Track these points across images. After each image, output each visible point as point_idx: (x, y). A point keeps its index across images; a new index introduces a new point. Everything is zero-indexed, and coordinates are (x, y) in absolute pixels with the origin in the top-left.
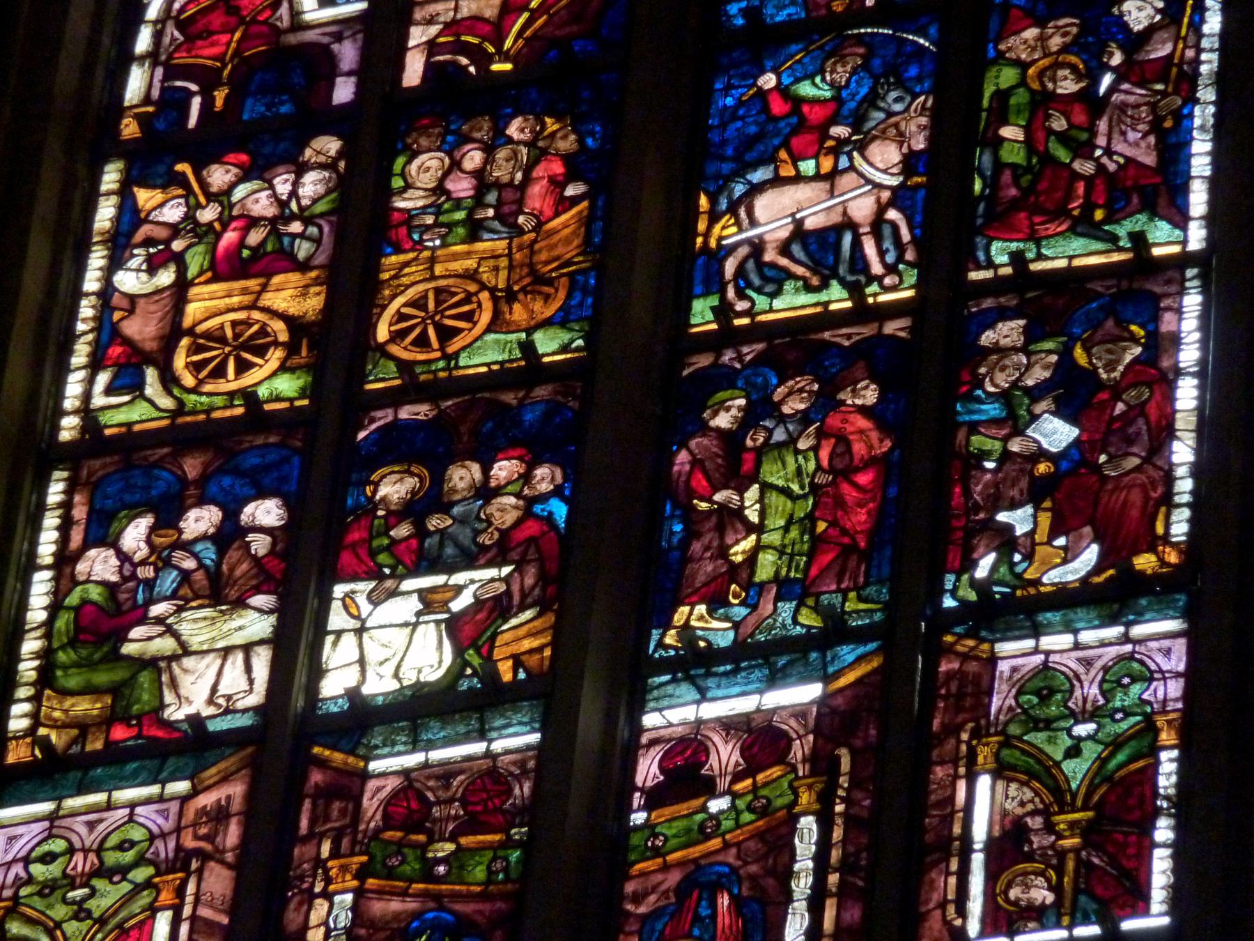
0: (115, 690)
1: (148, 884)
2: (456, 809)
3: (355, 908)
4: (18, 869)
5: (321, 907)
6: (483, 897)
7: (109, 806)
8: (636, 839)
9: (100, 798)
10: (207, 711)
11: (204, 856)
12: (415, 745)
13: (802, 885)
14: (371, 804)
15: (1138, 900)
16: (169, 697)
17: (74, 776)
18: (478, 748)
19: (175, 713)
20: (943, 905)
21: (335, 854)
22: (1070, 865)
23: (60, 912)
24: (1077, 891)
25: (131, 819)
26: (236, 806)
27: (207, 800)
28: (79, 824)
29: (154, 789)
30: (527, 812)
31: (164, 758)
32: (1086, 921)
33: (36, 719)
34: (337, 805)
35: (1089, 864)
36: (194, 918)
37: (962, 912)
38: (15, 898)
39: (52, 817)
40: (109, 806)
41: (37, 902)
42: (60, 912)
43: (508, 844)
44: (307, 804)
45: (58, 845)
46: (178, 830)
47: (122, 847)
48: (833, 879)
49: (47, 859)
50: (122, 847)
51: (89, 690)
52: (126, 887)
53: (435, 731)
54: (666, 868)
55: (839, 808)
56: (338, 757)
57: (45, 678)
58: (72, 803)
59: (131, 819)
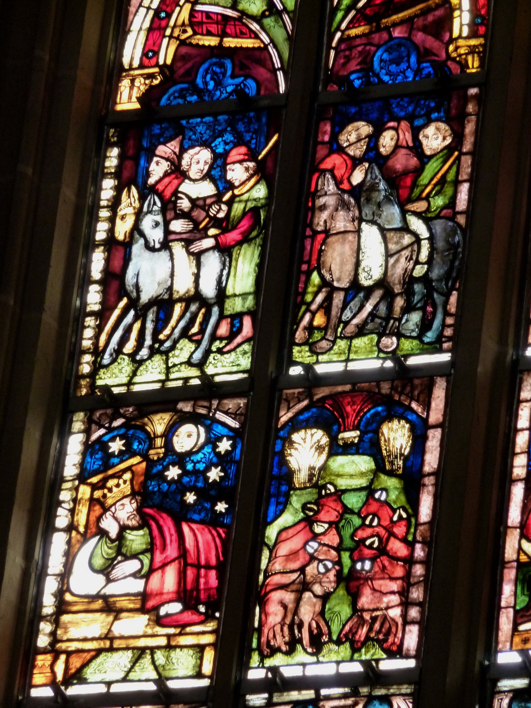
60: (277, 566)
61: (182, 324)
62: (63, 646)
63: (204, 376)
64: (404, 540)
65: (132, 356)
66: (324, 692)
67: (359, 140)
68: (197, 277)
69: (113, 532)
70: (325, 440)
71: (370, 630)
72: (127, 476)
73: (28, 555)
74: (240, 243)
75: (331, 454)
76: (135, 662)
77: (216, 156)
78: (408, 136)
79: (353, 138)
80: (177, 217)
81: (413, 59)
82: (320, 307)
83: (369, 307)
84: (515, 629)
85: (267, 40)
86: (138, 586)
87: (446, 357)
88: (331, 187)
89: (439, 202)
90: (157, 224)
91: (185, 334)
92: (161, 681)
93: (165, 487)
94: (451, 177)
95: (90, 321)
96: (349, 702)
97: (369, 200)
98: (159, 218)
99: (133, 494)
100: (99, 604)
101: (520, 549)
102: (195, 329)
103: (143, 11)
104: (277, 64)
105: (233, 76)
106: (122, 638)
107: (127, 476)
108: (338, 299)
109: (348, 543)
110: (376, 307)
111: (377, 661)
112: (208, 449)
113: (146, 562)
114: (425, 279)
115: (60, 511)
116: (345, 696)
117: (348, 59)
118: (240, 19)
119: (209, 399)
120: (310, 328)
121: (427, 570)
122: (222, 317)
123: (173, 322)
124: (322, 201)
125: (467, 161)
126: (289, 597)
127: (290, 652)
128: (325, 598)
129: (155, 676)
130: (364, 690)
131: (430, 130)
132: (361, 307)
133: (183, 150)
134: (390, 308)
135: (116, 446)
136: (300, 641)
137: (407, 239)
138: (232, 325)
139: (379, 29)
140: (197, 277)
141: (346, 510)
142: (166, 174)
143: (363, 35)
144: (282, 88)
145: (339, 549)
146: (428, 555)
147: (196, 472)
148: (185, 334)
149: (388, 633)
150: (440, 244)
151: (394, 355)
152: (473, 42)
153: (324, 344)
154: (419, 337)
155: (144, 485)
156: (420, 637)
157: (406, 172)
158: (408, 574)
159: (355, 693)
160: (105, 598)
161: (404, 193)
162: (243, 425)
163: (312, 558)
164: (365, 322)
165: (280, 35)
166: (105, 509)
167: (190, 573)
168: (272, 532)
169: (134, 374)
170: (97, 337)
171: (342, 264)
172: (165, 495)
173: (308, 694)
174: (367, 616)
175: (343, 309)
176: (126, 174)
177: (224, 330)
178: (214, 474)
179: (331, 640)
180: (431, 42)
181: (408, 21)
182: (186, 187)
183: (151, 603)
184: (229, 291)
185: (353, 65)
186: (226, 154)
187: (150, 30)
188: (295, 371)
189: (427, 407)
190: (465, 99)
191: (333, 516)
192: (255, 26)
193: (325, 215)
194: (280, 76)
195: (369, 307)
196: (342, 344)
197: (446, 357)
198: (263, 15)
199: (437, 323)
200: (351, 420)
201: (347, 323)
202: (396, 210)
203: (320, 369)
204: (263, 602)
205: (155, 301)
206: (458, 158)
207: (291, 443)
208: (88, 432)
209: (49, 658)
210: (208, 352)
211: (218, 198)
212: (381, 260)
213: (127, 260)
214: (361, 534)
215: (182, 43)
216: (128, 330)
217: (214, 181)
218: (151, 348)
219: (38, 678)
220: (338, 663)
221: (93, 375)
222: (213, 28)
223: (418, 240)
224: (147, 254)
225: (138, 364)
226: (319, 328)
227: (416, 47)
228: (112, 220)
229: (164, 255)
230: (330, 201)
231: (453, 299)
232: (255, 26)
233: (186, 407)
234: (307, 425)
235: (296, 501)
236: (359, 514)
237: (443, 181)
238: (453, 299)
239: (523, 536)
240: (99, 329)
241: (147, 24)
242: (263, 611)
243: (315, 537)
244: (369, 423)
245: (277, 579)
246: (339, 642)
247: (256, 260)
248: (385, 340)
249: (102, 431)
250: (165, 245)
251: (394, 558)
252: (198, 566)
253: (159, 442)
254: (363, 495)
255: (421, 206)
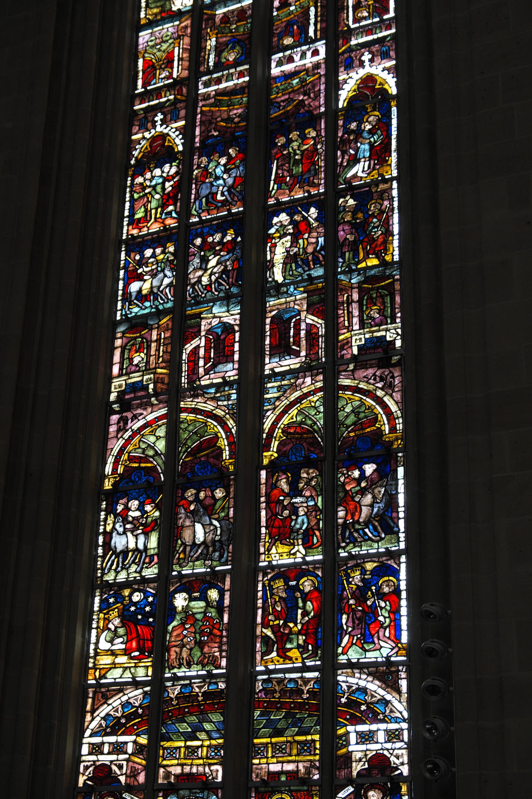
0: (162, 6)
1: (173, 43)
2: (236, 18)
3: (216, 41)
4: (146, 44)
5: (209, 42)
6: (243, 34)
7: (163, 29)
8: (275, 18)
9: (161, 28)
10: (181, 7)
11: (183, 36)
12: (225, 7)
13: (312, 21)
14: (217, 20)
15: (387, 11)
16: (173, 6)
17: (154, 25)
18: (239, 5)
19: (174, 8)
20: (344, 20)
21: (211, 31)
22: (371, 7)
23: (155, 51)
24: (373, 12)
25: (168, 31)
26: (189, 25)
27: (183, 25)
28: (157, 34)
29: (172, 24)
30: (251, 16)
31: (173, 18)
32: (376, 17)
33: (146, 14)
34: (210, 22)
35: (376, 7)
36: (183, 48)
37: (348, 20)
38: (146, 50)
39: (151, 33)
40: (163, 29)
41: (151, 50)
42: (155, 51)
43: (248, 23)
44: (204, 22)
45: (153, 38)
46: (178, 31)
47: (166, 36)
48: (319, 19)
49: (151, 41)
50: (166, 36)
51: (157, 7)
52: (168, 44)
53: (229, 3)
54: (282, 22)
55: (319, 4)
56: (209, 12)
57: (147, 6)
58: (155, 29)
59: (168, 31)
60: (173, 639)
61: (132, 559)
62: (98, 667)
63: (141, 576)
64: (219, 630)
65: (115, 570)
66: (193, 681)
67: (192, 495)
68: (136, 543)
69: (113, 629)
70: (187, 596)
71: (208, 660)
72: (116, 610)
73: (83, 636)
74: (151, 531)
75: (189, 602)
76: (124, 672)
77: (140, 503)
78: (210, 493)
79: (189, 494)
80: (128, 523)
81: (209, 467)
82: (182, 551)
83: (200, 551)
84: (262, 659)
85: (156, 463)
86: (123, 646)
87: (229, 567)
88: (183, 511)
89: (223, 514)
90: (121, 526)
91: (133, 562)
92: (134, 678)
93: (130, 613)
94: (227, 506)
95: (99, 559)
96: (202, 684)
97: (197, 515)
98: (121, 524)
99: (119, 616)
100: (109, 653)
101: (262, 632)
102: (137, 561)
103: (111, 457)
104: (160, 471)
105: (145, 476)
106: (118, 664)
107: (116, 610)
108: (188, 549)
109: (198, 631)
110: (202, 551)
111: (212, 670)
112: (144, 601)
113: (125, 638)
114: (219, 541)
115: (94, 622)
116: (200, 682)
117: (186, 468)
118: (145, 457)
119: (144, 584)
120: (179, 559)
121: (228, 639)
122: (146, 556)
123: (129, 558)
124: (180, 516)
125: (232, 501)
126: (178, 650)
127: (179, 668)
128: (191, 649)
129: (131, 676)
130: (208, 680)
131: (218, 491)
132: (197, 551)
133: (129, 501)
134: (208, 551)
135: (111, 600)
136: (183, 664)
137: (212, 528)
138: (150, 559)
139: (196, 458)
140: (136, 543)
141: (197, 620)
142: (123, 509)
143: (190, 460)
144: (163, 479)
145: (195, 633)
146: (228, 634)
147: (141, 608)
148: (133, 562)
149: (215, 660)
150: (225, 529)
151: (210, 567)
152: (231, 461)
153: (184, 564)
154: (219, 560)
155: (122, 613)
156: (227, 662)
157: (210, 505)
158: (221, 641)
159: (204, 681)
160: (112, 651)
161: (209, 512)
162: (156, 592)
163: (185, 636)
164: (199, 556)
165: (160, 462)
166: (110, 621)
167: (141, 642)
168: (170, 628)
169: (116, 576)
170: (102, 564)
171: (190, 537)
172: (130, 616)
173: (187, 682)
174: (207, 655)
175: (190, 552)
176: (109, 510)
177: (147, 560)
178: (148, 609)
179: (194, 664)
180: (216, 461)
181: (207, 455)
182: (130, 513)
183: (127, 653)
184: (149, 547)
185: (188, 471)
186: (144, 502)
187: (114, 463)
188: (174, 573)
189: (224, 584)
190: (230, 480)
191: (192, 622)
192: (151, 459)
193: (181, 521)
194: (162, 475)
195: (200, 551)
196: (191, 564)
197: (230, 567)
198: (154, 455)
199: (225, 556)
200: (196, 589)
201: (192, 557)
202: (207, 518)
203: (183, 572)
204: (168, 651)
205: (122, 552)
206: (229, 500)
207: (175, 598)
208: (101, 596)
209: (93, 670)
210: (142, 568)
211: (142, 517)
212: (203, 535)
213: (111, 538)
214: (203, 628)
215: (126, 466)
216: (113, 561)
217: (140, 511)
218: (122, 567)
219: (90, 677)
220: (197, 671)
221: (102, 576)
222: (136, 461)
223: (216, 527)
224: (118, 536)
225: (117, 573)
226: (182, 559)
227: (210, 463)
228: (105, 525)
229: (124, 536)
230: (183, 516)
231: (231, 547)
232: (151, 459)
233: (136, 587)
234: (180, 591)
235: (178, 617)
236: (201, 621)
237: (223, 508)
238: (231, 547)
239: (262, 627)
240: (103, 562)
241: (113, 461)
242: (169, 655)
243: (186, 629)
244: (202, 590)
245: (173, 643)
246: (197, 664)
247: (157, 536)
248: (207, 562)
249: (106, 595)
250: (124, 533)
251: (216, 636)
252: (144, 640)
253: (127, 598)
254: (202, 615)
255: (216, 516)
